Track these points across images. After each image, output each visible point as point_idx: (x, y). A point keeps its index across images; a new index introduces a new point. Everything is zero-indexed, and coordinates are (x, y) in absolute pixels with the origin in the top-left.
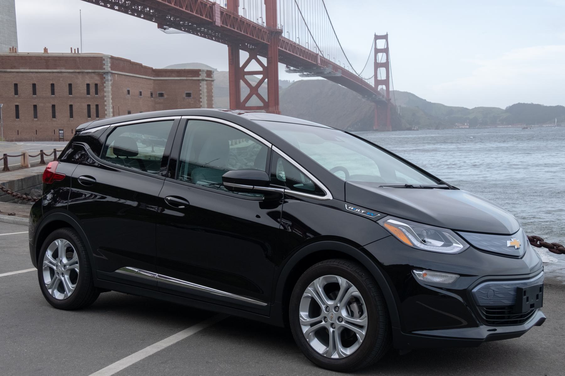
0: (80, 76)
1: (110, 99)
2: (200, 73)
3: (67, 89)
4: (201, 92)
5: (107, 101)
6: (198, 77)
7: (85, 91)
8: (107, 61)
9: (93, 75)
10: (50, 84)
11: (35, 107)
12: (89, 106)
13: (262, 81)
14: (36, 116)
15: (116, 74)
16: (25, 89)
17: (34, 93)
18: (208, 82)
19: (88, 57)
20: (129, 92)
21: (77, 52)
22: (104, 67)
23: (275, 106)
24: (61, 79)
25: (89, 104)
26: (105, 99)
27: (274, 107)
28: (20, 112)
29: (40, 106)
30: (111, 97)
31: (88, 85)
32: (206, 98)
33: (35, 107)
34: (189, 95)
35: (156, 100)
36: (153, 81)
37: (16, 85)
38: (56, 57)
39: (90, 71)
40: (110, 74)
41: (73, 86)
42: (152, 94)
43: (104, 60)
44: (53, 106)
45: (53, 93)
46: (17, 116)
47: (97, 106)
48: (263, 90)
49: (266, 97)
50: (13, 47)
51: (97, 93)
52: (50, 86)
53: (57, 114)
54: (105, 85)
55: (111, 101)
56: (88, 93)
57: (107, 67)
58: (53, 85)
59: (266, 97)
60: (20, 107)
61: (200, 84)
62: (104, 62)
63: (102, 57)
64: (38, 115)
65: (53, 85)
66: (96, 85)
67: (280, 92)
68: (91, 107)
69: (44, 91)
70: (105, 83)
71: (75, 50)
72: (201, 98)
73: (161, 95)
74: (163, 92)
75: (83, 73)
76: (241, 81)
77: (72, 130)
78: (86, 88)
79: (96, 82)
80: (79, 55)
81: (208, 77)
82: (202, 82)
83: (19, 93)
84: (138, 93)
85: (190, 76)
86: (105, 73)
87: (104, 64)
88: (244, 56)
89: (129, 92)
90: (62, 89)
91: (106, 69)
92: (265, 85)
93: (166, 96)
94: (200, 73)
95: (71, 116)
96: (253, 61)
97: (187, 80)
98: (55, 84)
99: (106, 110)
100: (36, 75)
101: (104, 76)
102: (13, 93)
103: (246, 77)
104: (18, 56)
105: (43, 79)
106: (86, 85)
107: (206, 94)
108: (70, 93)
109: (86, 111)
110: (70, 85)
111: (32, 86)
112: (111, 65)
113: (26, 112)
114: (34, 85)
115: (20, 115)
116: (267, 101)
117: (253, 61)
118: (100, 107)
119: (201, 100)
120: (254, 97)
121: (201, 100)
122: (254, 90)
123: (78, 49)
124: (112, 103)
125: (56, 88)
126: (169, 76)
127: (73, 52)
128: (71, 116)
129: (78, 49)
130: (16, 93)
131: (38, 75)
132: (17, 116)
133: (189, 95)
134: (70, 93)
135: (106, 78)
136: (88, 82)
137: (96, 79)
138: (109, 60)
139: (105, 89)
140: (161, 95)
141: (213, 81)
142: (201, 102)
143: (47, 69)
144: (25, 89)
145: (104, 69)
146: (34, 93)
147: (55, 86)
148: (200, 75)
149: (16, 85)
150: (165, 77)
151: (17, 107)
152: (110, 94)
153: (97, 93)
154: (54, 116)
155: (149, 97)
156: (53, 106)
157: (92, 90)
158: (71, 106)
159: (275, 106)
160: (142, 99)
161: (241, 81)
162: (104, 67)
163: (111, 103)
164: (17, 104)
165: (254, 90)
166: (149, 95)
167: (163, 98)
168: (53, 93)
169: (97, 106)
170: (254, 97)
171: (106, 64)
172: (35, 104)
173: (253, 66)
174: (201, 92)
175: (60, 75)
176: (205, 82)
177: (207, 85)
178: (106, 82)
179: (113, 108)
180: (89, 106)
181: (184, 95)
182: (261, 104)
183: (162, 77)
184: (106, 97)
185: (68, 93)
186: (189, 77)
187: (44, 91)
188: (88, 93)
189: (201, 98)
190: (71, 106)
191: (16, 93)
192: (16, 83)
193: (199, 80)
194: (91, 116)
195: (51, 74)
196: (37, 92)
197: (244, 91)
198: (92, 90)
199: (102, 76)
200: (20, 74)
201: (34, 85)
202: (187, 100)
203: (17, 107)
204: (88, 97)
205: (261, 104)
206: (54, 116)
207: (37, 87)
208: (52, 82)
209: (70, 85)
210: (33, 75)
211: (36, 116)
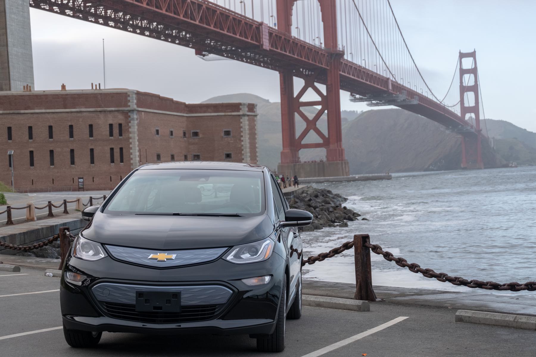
0: (102, 116)
1: (136, 140)
2: (241, 107)
3: (87, 131)
4: (242, 129)
5: (133, 143)
6: (239, 111)
7: (108, 133)
8: (133, 97)
9: (116, 113)
10: (68, 125)
11: (52, 152)
12: (112, 149)
13: (321, 113)
14: (52, 163)
15: (143, 111)
16: (41, 133)
17: (51, 136)
18: (250, 117)
19: (111, 93)
20: (157, 132)
21: (98, 88)
22: (129, 104)
23: (337, 142)
24: (81, 120)
25: (113, 147)
26: (131, 140)
27: (336, 144)
28: (35, 159)
29: (57, 150)
30: (137, 138)
31: (111, 126)
32: (248, 136)
33: (52, 152)
34: (227, 133)
35: (190, 141)
36: (186, 118)
37: (30, 128)
38: (75, 94)
39: (113, 109)
40: (135, 112)
41: (94, 127)
42: (185, 134)
43: (129, 96)
44: (72, 151)
45: (71, 135)
46: (32, 164)
47: (121, 149)
48: (323, 124)
49: (325, 132)
50: (27, 85)
51: (121, 134)
52: (68, 127)
53: (76, 160)
54: (130, 124)
55: (137, 143)
56: (111, 134)
57: (133, 104)
58: (71, 127)
59: (325, 132)
60: (34, 153)
61: (241, 120)
62: (129, 98)
63: (127, 93)
64: (55, 162)
65: (71, 127)
66: (120, 125)
67: (344, 127)
68: (115, 150)
69: (61, 134)
70: (130, 122)
71: (96, 85)
72: (242, 136)
73: (196, 134)
74: (198, 131)
75: (105, 111)
76: (296, 114)
77: (93, 178)
78: (108, 129)
79: (120, 122)
80: (100, 92)
81: (251, 112)
82: (243, 118)
83: (34, 137)
84: (169, 133)
85: (229, 111)
86: (130, 111)
87: (129, 100)
88: (298, 83)
89: (157, 132)
90: (81, 131)
91: (131, 106)
92: (324, 117)
93: (201, 136)
94: (241, 107)
95: (92, 162)
96: (310, 90)
97: (225, 115)
98: (74, 126)
99: (131, 154)
100: (52, 116)
101: (129, 114)
102: (27, 137)
103: (302, 109)
104: (33, 95)
105: (60, 120)
106: (108, 126)
107: (247, 132)
108: (91, 135)
109: (108, 155)
110: (91, 126)
111: (48, 128)
112: (137, 102)
113: (42, 159)
114: (50, 128)
115: (35, 162)
116: (327, 136)
117: (310, 90)
118: (124, 150)
119: (242, 139)
120: (312, 133)
121: (242, 139)
122: (311, 124)
123: (99, 84)
124: (138, 146)
125: (74, 130)
126: (205, 112)
127: (94, 88)
128: (92, 162)
129: (99, 84)
130: (31, 137)
131: (55, 116)
132: (32, 164)
133: (227, 133)
134: (91, 135)
135: (131, 116)
136: (111, 122)
137: (120, 119)
138: (134, 96)
139: (130, 130)
140: (196, 134)
141: (256, 116)
142: (242, 141)
143: (65, 108)
144: (41, 133)
145: (129, 106)
146: (51, 136)
147: (74, 127)
148: (240, 109)
149: (30, 128)
150: (201, 113)
151: (31, 153)
152: (136, 135)
153: (121, 134)
154: (73, 162)
155: (181, 137)
156: (72, 151)
157: (116, 131)
158: (92, 150)
159: (337, 142)
160: (173, 139)
161: (296, 114)
162: (129, 104)
163: (137, 146)
164: (31, 149)
165: (311, 124)
166: (182, 135)
167: (198, 137)
168: (71, 135)
169: (121, 149)
170: (312, 133)
171: (131, 101)
172: (51, 149)
173: (310, 96)
174: (242, 129)
175: (79, 115)
176: (246, 118)
177: (249, 120)
178: (132, 122)
179: (140, 151)
180: (112, 149)
181: (223, 134)
182: (320, 141)
183: (196, 112)
184: (131, 139)
185: (88, 136)
186: (228, 112)
187: (61, 134)
188: (111, 134)
189: (242, 136)
190: (92, 150)
191: (31, 137)
192: (30, 125)
193: (239, 115)
194: (115, 161)
195: (69, 115)
196: (54, 136)
197: (300, 125)
198: (116, 131)
199: (127, 114)
200: (35, 116)
201: (50, 128)
202: (226, 139)
203: (31, 153)
204: (111, 139)
205: (320, 141)
206: (73, 162)
207: (54, 129)
208: (70, 124)
209: (91, 126)
210: (49, 116)
211: (52, 163)
